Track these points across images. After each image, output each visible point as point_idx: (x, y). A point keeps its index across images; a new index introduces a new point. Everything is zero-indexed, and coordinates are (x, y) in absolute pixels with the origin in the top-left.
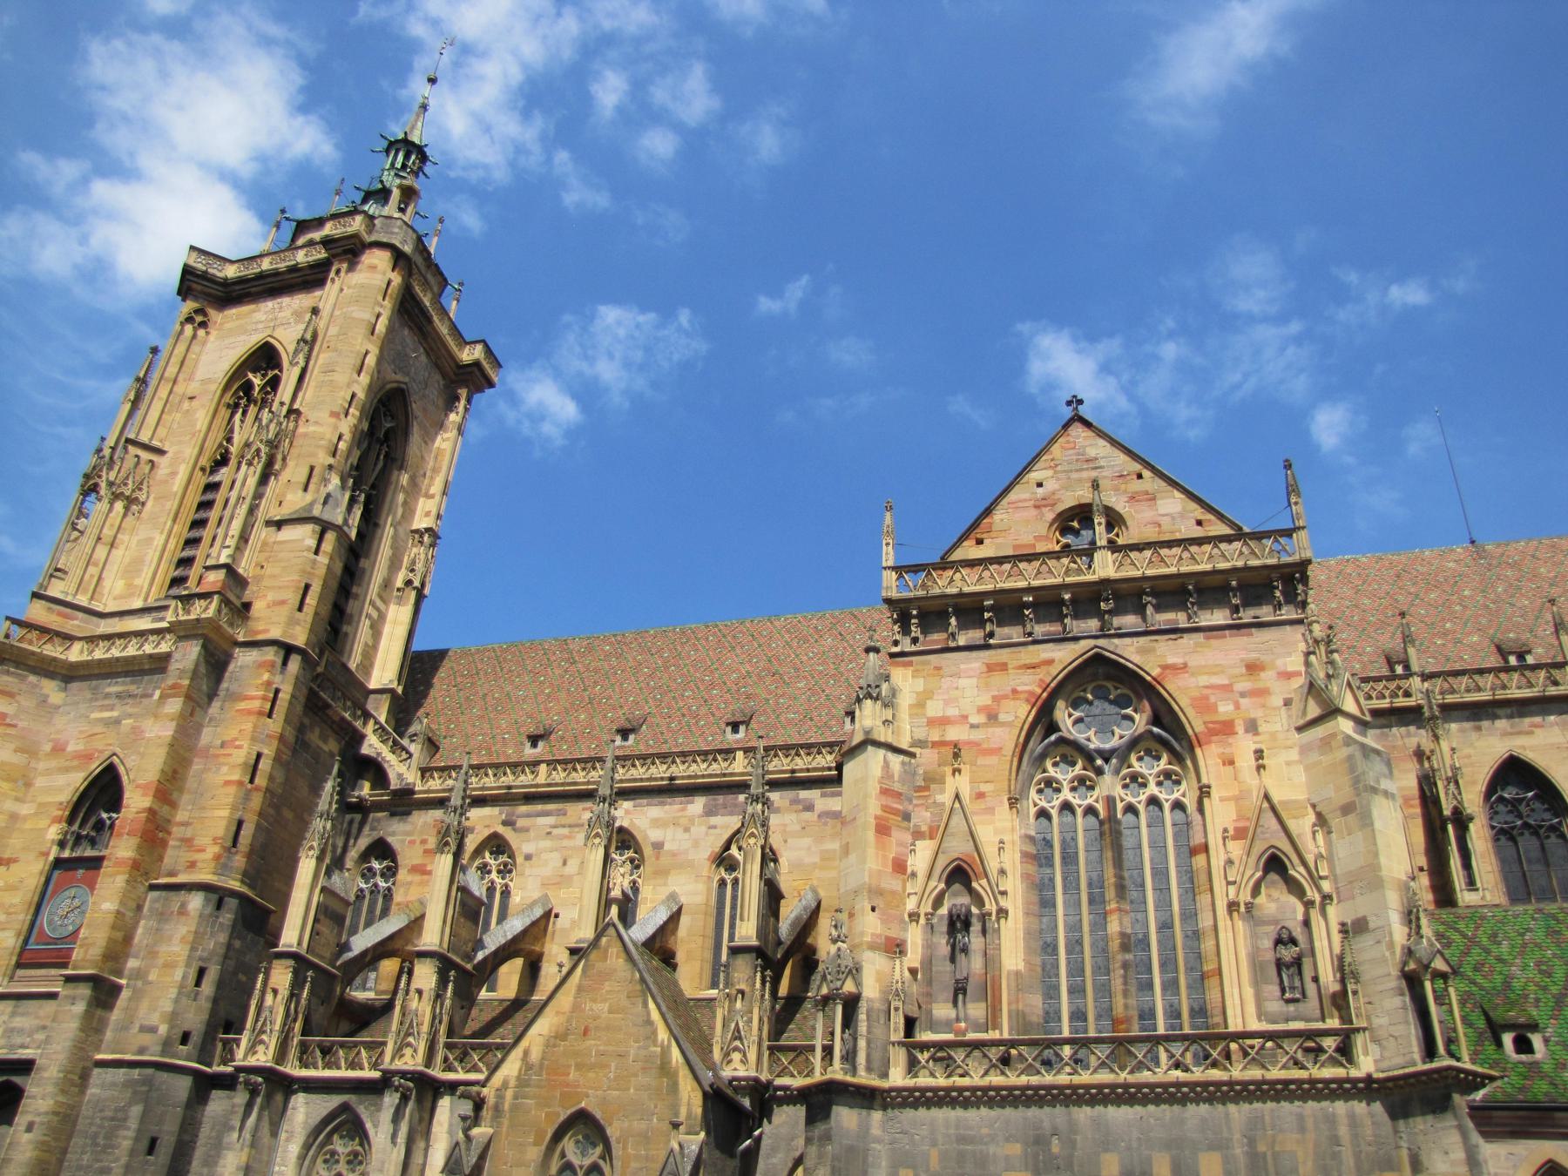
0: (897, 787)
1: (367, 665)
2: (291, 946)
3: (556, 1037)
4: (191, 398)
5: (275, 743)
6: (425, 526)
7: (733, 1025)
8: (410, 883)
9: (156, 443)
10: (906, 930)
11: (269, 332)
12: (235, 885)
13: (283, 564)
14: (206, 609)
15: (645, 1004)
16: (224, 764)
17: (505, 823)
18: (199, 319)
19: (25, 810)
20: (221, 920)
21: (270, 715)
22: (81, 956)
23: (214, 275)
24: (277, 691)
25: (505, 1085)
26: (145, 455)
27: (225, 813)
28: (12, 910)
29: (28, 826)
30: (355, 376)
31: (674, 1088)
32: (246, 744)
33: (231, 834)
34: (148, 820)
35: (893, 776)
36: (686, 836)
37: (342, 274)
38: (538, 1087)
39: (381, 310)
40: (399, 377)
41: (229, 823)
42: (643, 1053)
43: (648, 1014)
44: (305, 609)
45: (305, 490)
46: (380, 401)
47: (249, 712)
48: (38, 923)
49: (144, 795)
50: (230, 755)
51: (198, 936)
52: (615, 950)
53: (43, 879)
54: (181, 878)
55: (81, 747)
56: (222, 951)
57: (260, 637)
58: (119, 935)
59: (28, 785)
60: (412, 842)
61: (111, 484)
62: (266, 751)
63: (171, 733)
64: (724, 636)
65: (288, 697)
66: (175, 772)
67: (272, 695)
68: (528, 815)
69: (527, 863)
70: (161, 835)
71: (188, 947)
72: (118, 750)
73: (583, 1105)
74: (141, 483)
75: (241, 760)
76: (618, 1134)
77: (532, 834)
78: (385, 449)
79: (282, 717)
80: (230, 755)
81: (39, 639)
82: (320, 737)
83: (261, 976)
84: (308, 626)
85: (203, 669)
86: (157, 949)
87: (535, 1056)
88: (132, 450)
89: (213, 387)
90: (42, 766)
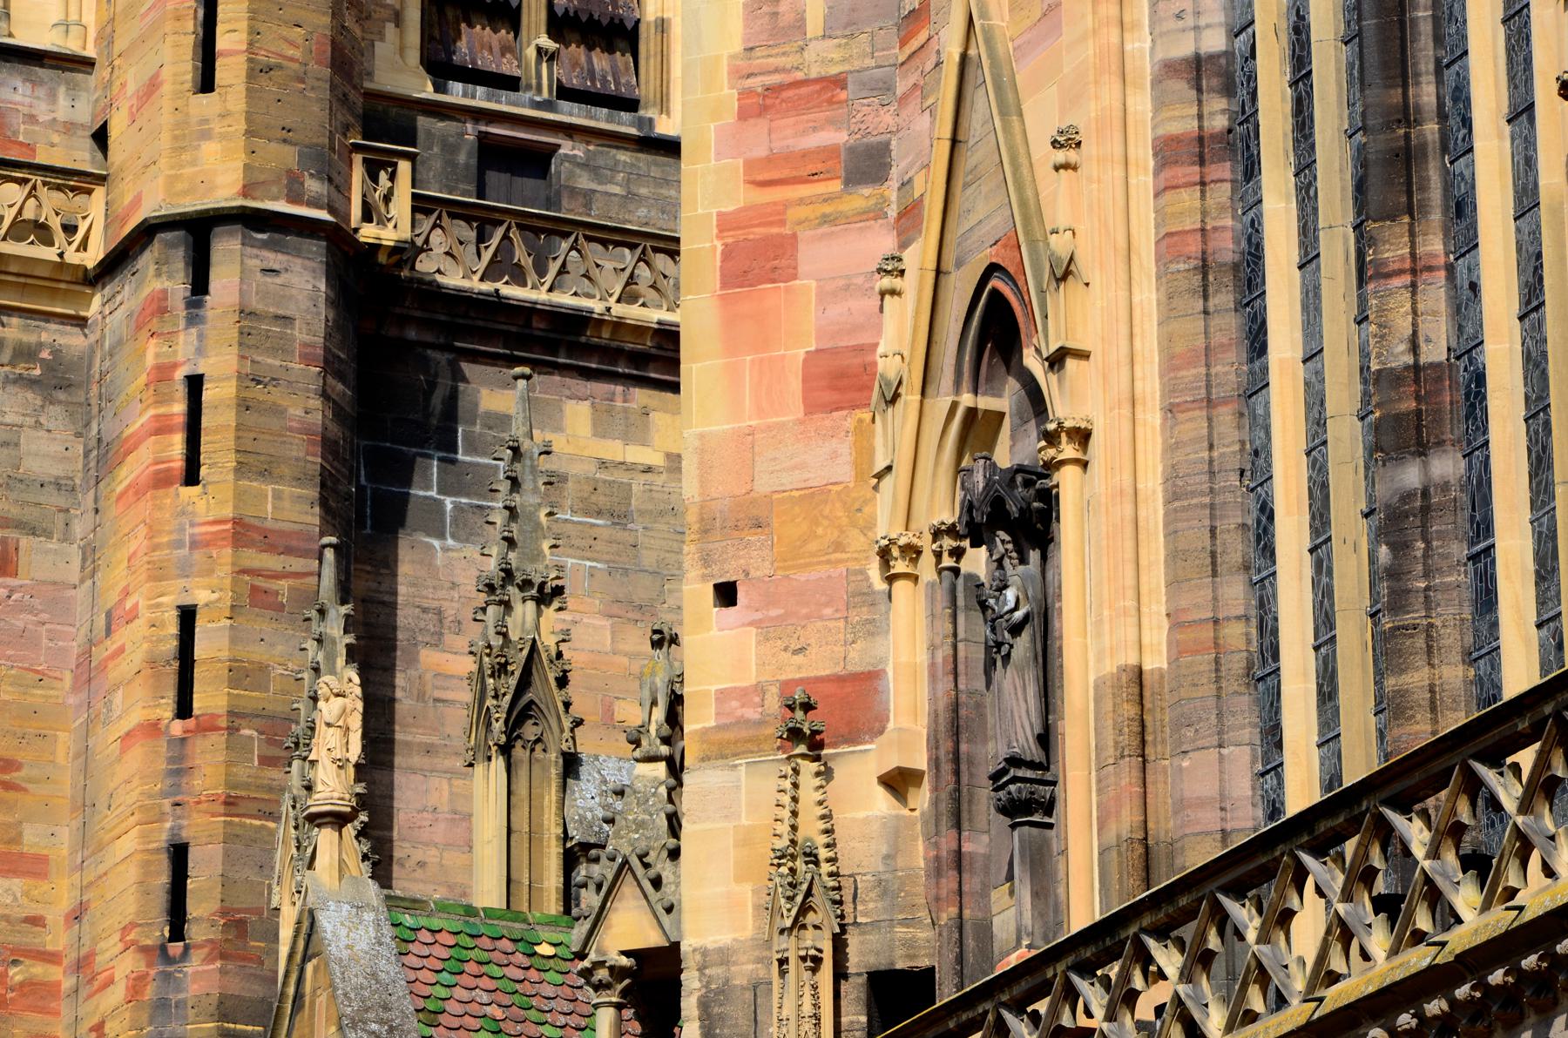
0: (822, 58)
10: (874, 629)
16: (116, 687)
21: (191, 476)
24: (195, 384)
27: (128, 844)
33: (160, 901)
35: (800, 24)
47: (137, 491)
50: (121, 650)
62: (201, 596)
67: (179, 408)
70: (16, 974)
82: (600, 430)
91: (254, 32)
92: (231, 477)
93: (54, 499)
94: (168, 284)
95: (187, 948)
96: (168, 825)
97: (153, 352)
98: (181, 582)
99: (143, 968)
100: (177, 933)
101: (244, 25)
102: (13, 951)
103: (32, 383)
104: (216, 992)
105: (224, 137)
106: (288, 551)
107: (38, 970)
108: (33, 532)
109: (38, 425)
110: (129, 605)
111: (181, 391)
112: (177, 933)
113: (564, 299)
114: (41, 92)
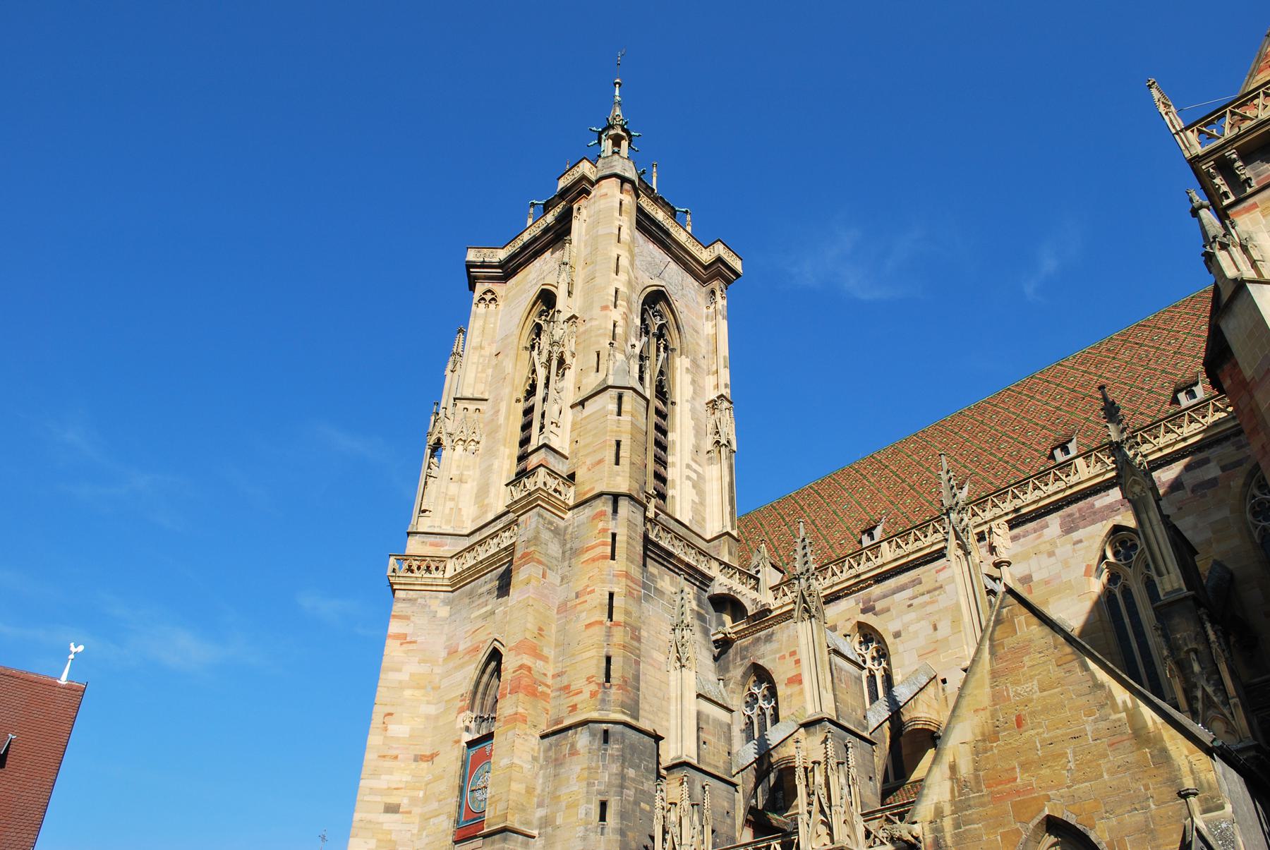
3: (984, 741)
7: (1199, 694)
8: (791, 695)
13: (593, 433)
15: (1085, 668)
16: (583, 611)
17: (864, 611)
18: (489, 297)
20: (610, 751)
21: (613, 558)
22: (492, 814)
24: (614, 536)
25: (939, 813)
26: (472, 406)
28: (442, 797)
31: (1163, 757)
33: (603, 671)
36: (1053, 559)
38: (983, 805)
39: (621, 223)
42: (1102, 725)
43: (1093, 676)
44: (621, 461)
45: (598, 371)
48: (464, 803)
52: (1022, 618)
54: (566, 723)
60: (783, 657)
62: (615, 590)
64: (1020, 393)
65: (625, 538)
66: (540, 629)
67: (610, 540)
68: (885, 596)
69: (898, 639)
70: (540, 689)
71: (584, 784)
73: (1047, 812)
76: (1106, 837)
77: (894, 612)
86: (558, 793)
87: (965, 769)
88: (461, 405)
92: (625, 560)
93: (556, 563)
94: (607, 509)
95: (611, 685)
96: (605, 650)
97: (601, 525)
98: (610, 585)
99: (597, 689)
100: (608, 680)
101: (629, 451)
102: (540, 682)
104: (620, 699)
106: (636, 584)
108: (550, 569)
109: (552, 542)
111: (611, 536)
112: (608, 680)
114: (557, 461)
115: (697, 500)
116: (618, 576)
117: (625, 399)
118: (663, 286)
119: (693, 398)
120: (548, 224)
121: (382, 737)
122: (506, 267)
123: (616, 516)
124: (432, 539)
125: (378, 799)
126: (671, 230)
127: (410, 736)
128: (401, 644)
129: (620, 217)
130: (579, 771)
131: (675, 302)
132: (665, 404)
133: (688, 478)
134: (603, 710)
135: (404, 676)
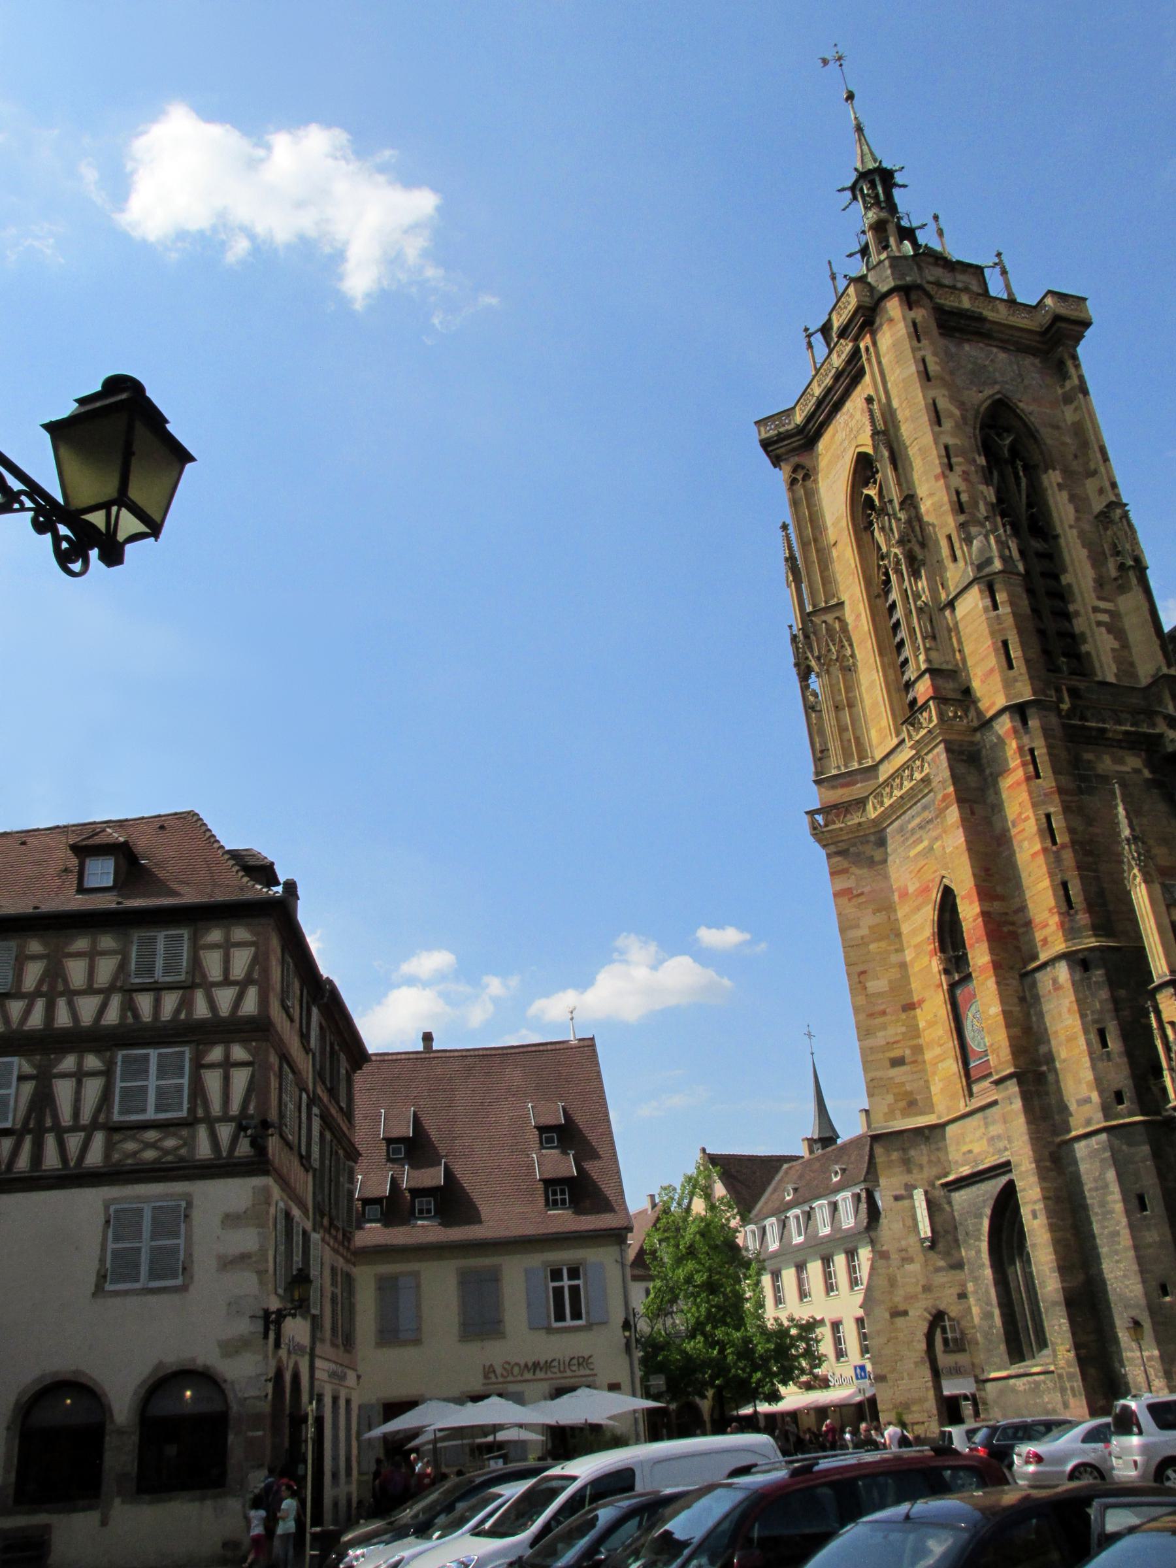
1: (1126, 666)
2: (1166, 975)
4: (835, 544)
5: (1056, 797)
6: (1104, 504)
9: (832, 603)
11: (854, 445)
12: (1091, 942)
14: (930, 717)
16: (1024, 840)
19: (909, 955)
21: (1038, 776)
23: (787, 431)
24: (1032, 751)
26: (829, 618)
27: (1046, 883)
28: (942, 1042)
29: (916, 969)
30: (937, 429)
32: (1030, 813)
33: (1063, 899)
34: (986, 923)
37: (871, 349)
39: (922, 353)
40: (988, 392)
41: (1054, 890)
46: (981, 429)
47: (1018, 784)
49: (971, 903)
50: (1024, 830)
51: (1082, 1005)
53: (949, 1007)
54: (1043, 957)
55: (917, 885)
56: (1110, 1006)
57: (989, 714)
58: (1017, 1031)
59: (898, 935)
61: (818, 658)
62: (1052, 810)
63: (963, 839)
65: (1044, 750)
66: (987, 870)
67: (1029, 758)
70: (1005, 929)
71: (1077, 1016)
72: (943, 873)
74: (841, 641)
75: (1034, 829)
78: (1019, 464)
79: (1050, 773)
80: (1023, 830)
81: (838, 816)
83: (1152, 1015)
84: (1026, 677)
85: (961, 769)
89: (844, 523)
90: (900, 914)
91: (1023, 651)
98: (1044, 807)
103: (965, 761)
105: (1022, 681)
107: (1011, 928)
110: (1023, 817)
111: (1028, 753)
113: (1100, 725)
115: (1116, 645)
116: (1051, 793)
117: (997, 587)
118: (998, 392)
119: (1077, 519)
120: (837, 368)
121: (864, 997)
122: (807, 430)
123: (1027, 728)
124: (842, 781)
125: (880, 1056)
126: (988, 314)
127: (892, 989)
128: (850, 900)
129: (920, 345)
130: (1068, 1005)
131: (1021, 405)
132: (1046, 540)
133: (1099, 624)
134: (1074, 939)
135: (864, 931)
